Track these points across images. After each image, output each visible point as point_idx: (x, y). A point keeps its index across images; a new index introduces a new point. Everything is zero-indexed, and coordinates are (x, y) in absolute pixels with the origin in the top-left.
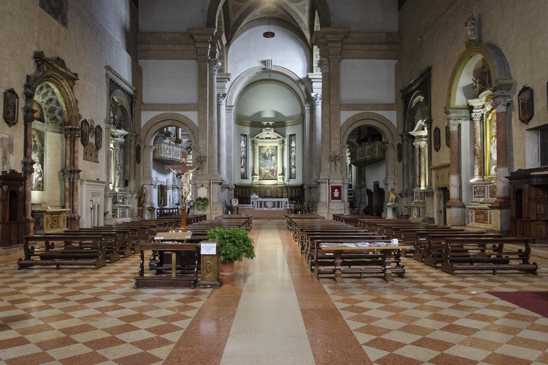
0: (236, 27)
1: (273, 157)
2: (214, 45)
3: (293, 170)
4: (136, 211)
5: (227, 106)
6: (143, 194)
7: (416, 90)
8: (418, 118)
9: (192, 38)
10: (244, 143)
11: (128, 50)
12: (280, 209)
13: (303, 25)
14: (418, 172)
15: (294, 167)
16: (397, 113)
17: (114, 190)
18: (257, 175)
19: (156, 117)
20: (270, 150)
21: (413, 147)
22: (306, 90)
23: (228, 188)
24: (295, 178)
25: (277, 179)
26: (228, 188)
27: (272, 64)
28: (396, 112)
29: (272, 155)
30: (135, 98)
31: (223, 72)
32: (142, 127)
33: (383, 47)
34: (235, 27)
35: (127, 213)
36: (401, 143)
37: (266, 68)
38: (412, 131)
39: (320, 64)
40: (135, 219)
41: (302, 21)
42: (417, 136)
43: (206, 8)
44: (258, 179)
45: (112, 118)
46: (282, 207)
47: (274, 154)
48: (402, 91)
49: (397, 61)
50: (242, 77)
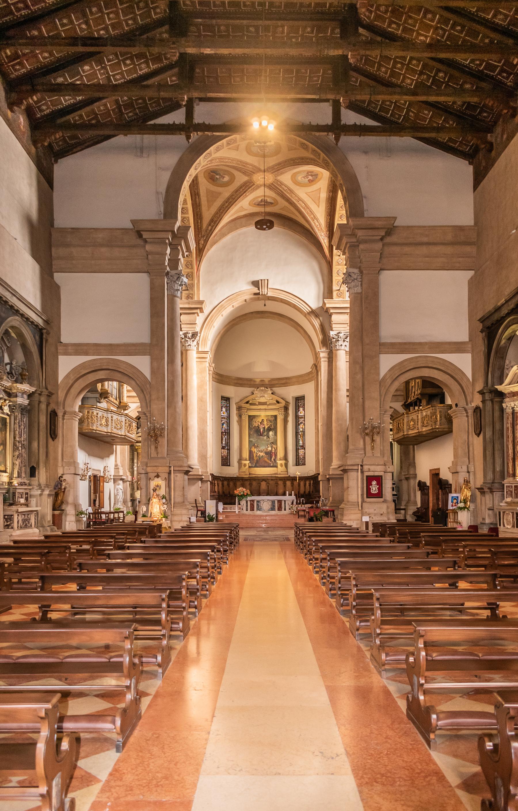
0: (212, 227)
1: (271, 433)
2: (175, 248)
3: (301, 452)
4: (49, 518)
5: (198, 352)
6: (61, 488)
7: (508, 315)
8: (510, 363)
9: (140, 236)
10: (226, 411)
11: (35, 254)
12: (283, 512)
13: (317, 224)
14: (511, 451)
15: (303, 447)
16: (472, 357)
17: (11, 483)
18: (246, 460)
19: (82, 366)
20: (265, 422)
21: (502, 410)
22: (322, 326)
23: (201, 480)
24: (304, 464)
25: (276, 467)
26: (201, 480)
27: (269, 287)
28: (470, 355)
29: (269, 429)
30: (48, 333)
31: (192, 298)
32: (59, 383)
33: (449, 250)
34: (210, 228)
35: (33, 521)
36: (481, 405)
38: (501, 384)
39: (348, 279)
40: (47, 530)
41: (315, 218)
42: (509, 394)
43: (163, 189)
44: (247, 467)
45: (7, 364)
46: (285, 510)
48: (482, 320)
49: (472, 273)
50: (222, 306)
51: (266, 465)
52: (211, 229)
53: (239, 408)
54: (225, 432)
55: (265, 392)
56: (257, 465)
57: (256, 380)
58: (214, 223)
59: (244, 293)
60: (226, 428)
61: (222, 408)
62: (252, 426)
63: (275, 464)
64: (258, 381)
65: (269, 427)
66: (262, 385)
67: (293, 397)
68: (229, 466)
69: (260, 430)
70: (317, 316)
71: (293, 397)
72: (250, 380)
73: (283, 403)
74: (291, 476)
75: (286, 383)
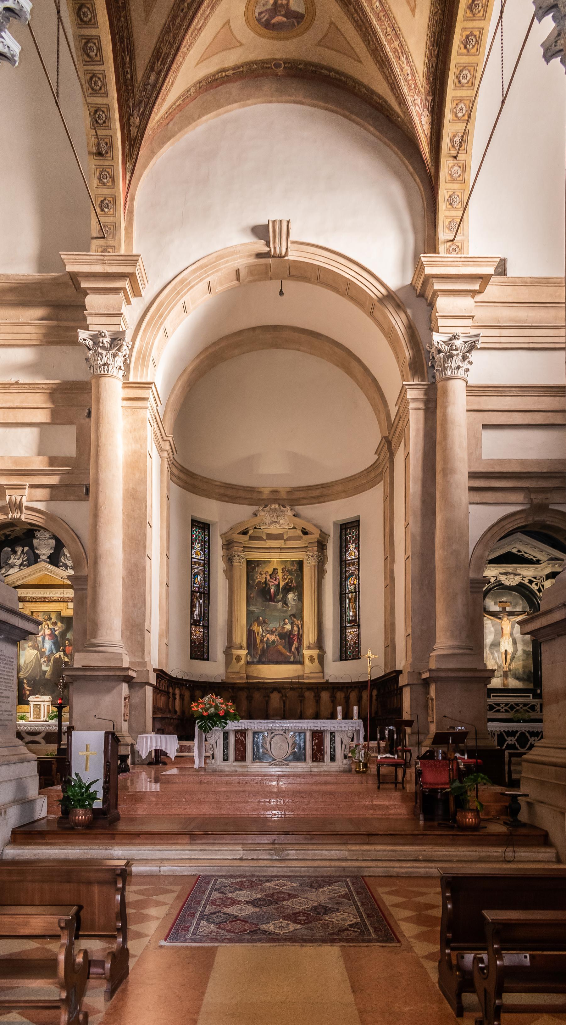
0: (159, 74)
1: (291, 596)
3: (351, 633)
5: (127, 385)
12: (327, 766)
13: (407, 68)
15: (356, 623)
18: (241, 648)
20: (280, 574)
22: (411, 330)
23: (128, 680)
25: (301, 663)
26: (128, 680)
27: (291, 238)
29: (287, 589)
34: (152, 78)
37: (269, 252)
41: (403, 51)
44: (243, 661)
46: (333, 759)
47: (294, 584)
50: (182, 281)
51: (281, 659)
52: (156, 82)
53: (228, 544)
54: (200, 593)
55: (280, 513)
56: (264, 659)
57: (263, 490)
58: (163, 64)
59: (234, 253)
60: (202, 584)
61: (192, 543)
62: (254, 581)
63: (298, 658)
64: (266, 492)
65: (287, 584)
66: (275, 501)
67: (335, 523)
68: (208, 659)
69: (270, 589)
70: (399, 306)
71: (335, 523)
72: (252, 490)
73: (315, 536)
74: (330, 681)
75: (322, 496)
